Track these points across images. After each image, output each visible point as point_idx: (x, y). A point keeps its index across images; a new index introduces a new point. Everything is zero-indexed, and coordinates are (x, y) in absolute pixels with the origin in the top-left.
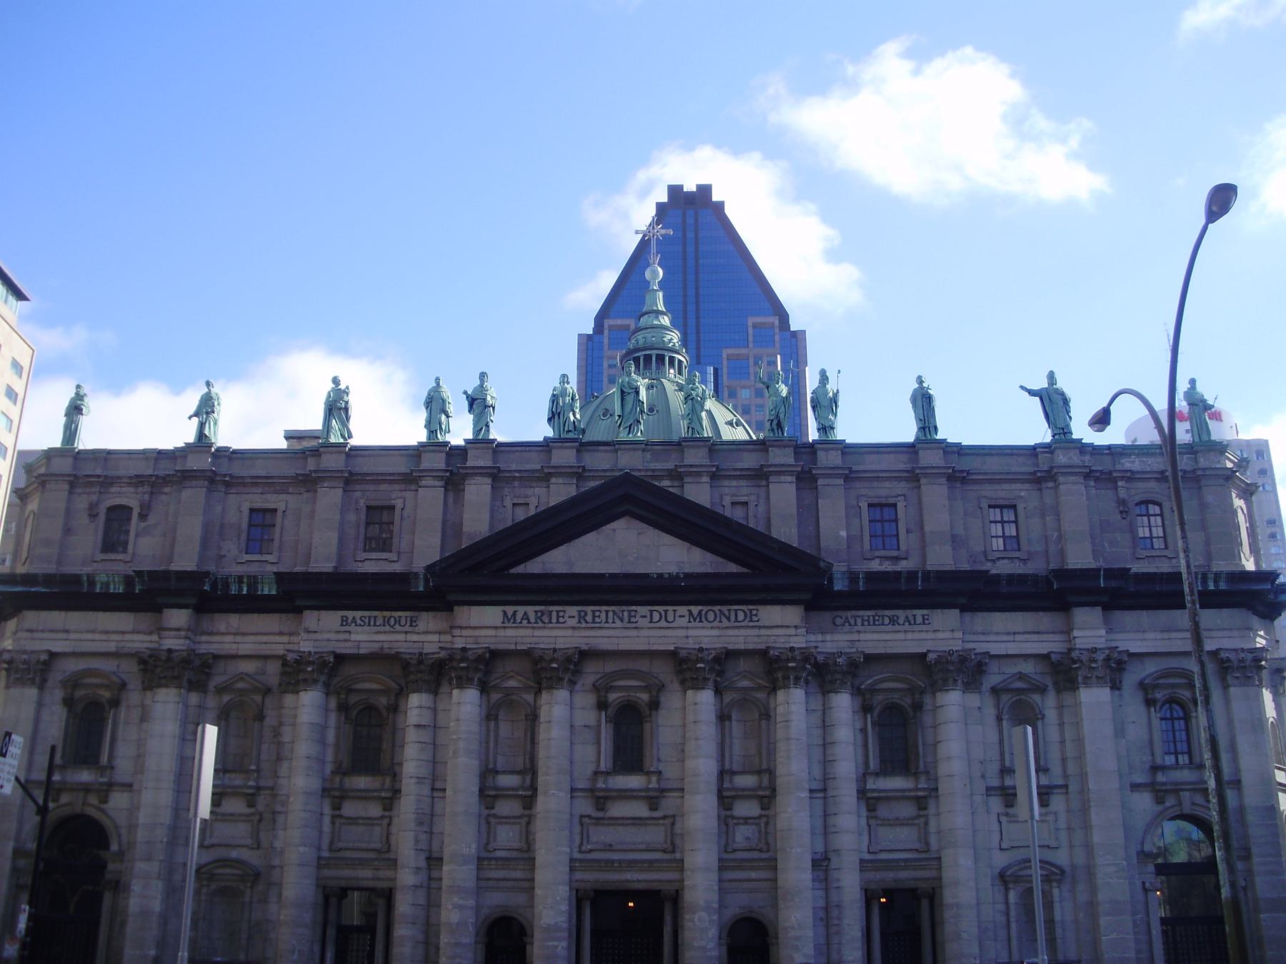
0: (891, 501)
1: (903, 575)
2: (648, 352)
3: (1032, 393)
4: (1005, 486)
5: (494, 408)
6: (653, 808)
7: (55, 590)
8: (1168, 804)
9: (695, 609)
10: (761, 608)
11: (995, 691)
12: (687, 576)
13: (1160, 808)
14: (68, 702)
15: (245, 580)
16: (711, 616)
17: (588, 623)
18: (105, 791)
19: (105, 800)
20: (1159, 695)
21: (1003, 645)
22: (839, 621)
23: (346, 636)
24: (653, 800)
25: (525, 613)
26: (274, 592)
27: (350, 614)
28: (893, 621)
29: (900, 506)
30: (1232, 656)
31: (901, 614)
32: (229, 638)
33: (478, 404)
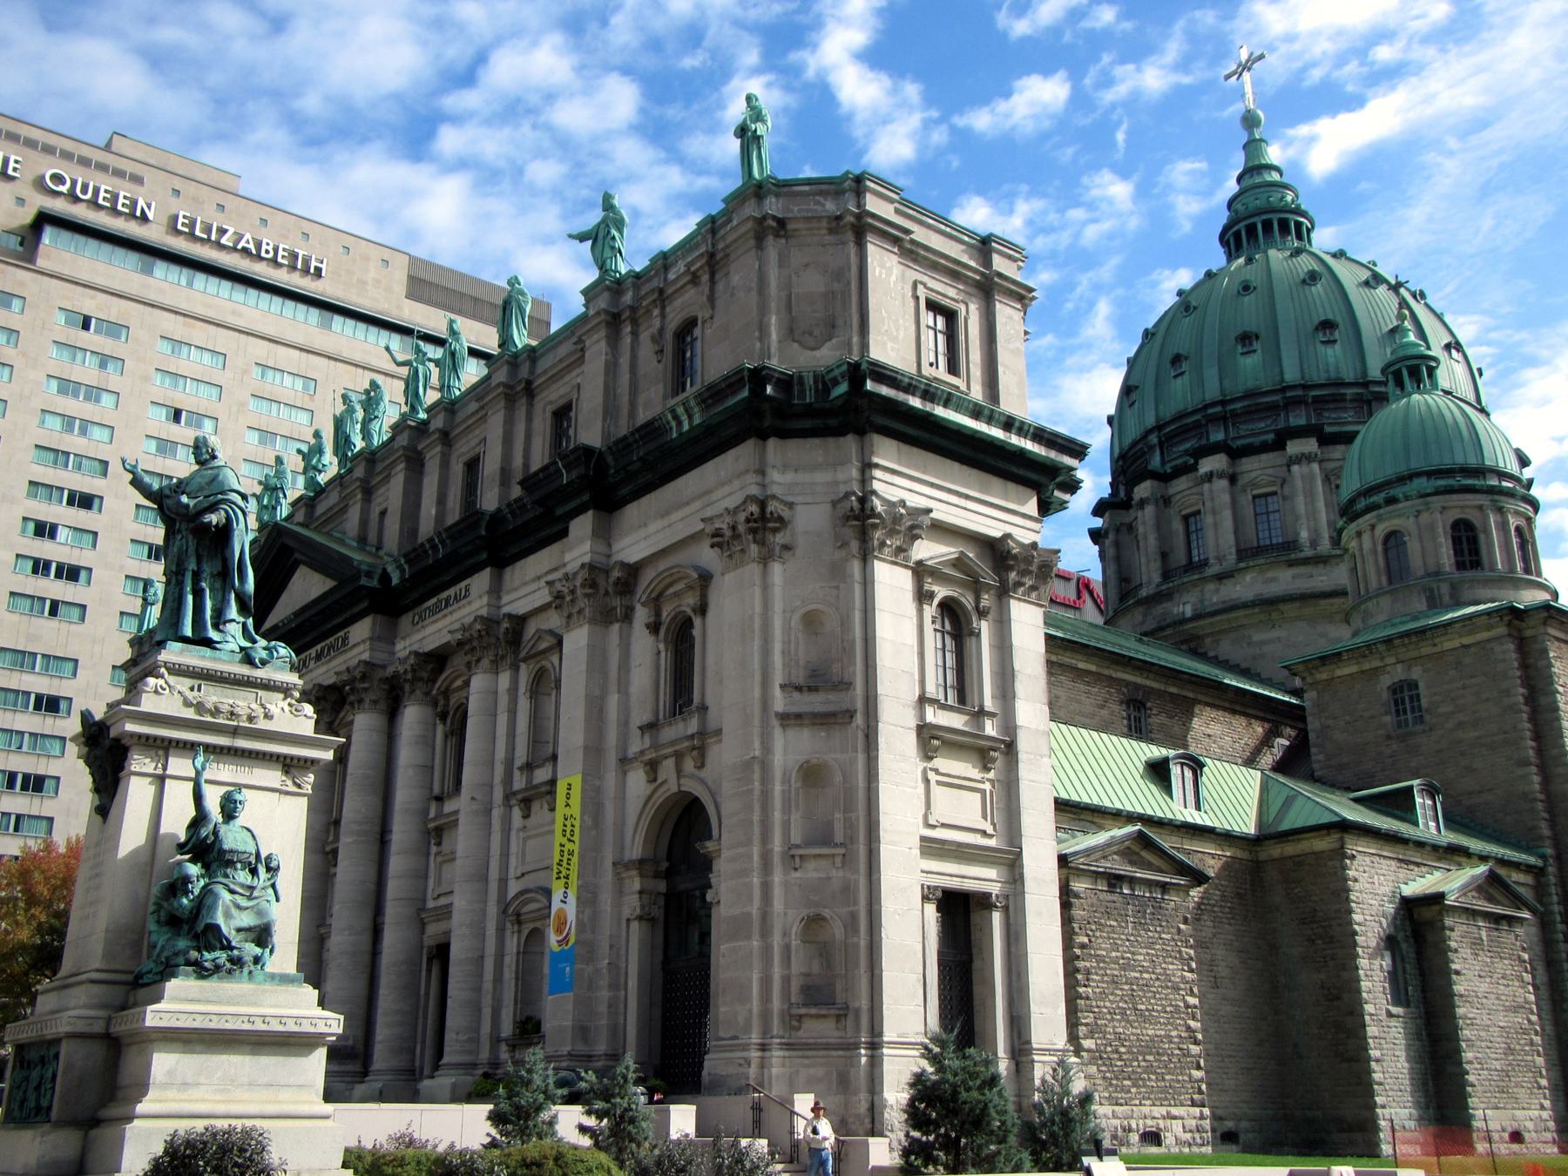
0: (477, 450)
1: (427, 546)
2: (1236, 228)
3: (582, 238)
4: (567, 378)
5: (282, 488)
8: (659, 781)
9: (319, 647)
10: (350, 629)
12: (297, 614)
13: (653, 786)
20: (667, 613)
21: (530, 598)
22: (417, 618)
30: (723, 524)
31: (451, 592)
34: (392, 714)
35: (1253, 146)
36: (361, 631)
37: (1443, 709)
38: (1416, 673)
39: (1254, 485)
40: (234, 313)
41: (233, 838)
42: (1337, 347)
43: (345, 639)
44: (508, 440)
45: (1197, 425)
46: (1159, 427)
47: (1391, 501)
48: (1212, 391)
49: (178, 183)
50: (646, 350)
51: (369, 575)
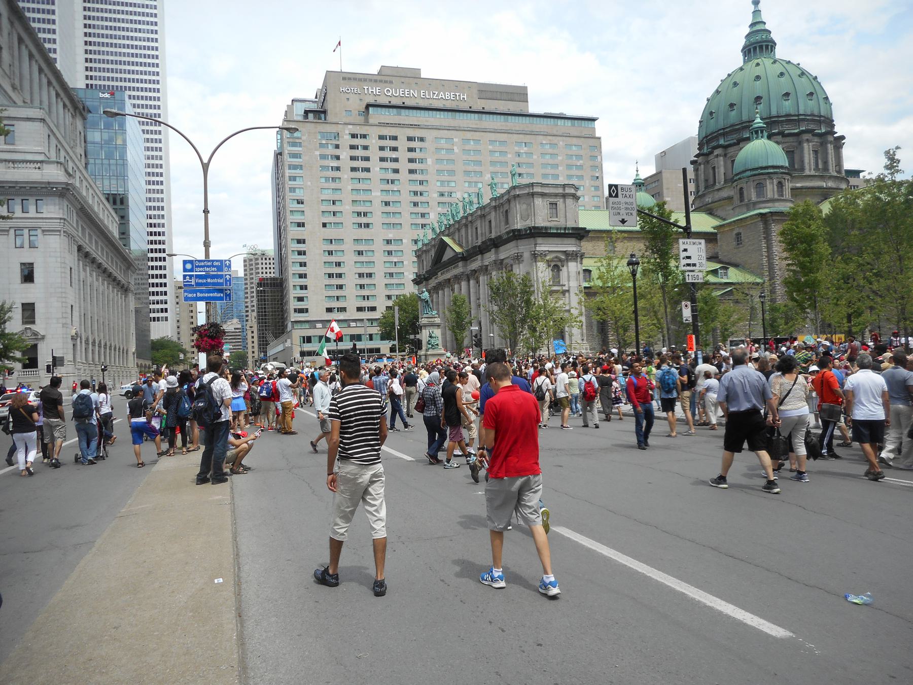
34: (469, 281)
35: (757, 12)
36: (460, 264)
37: (746, 241)
38: (741, 231)
39: (731, 157)
40: (427, 121)
41: (433, 335)
42: (762, 105)
44: (481, 227)
45: (716, 137)
46: (706, 137)
47: (740, 179)
48: (721, 125)
49: (403, 80)
50: (501, 214)
51: (460, 254)
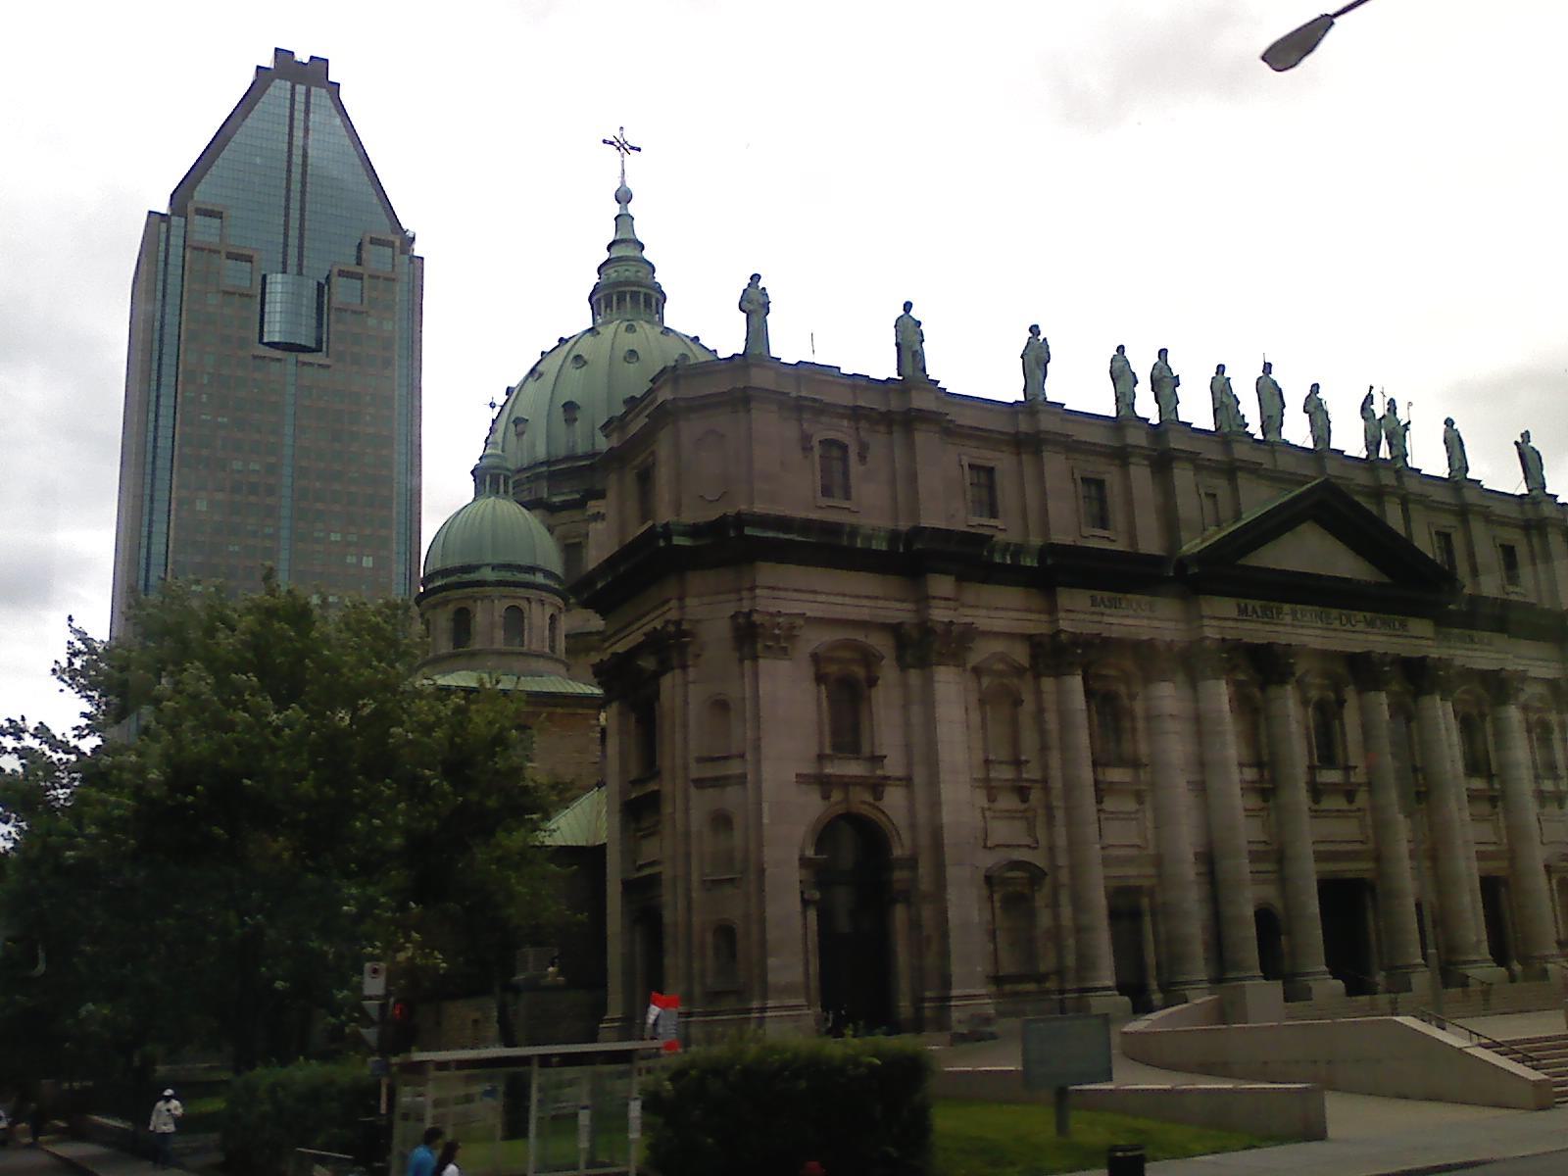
0: (1447, 530)
6: (1351, 801)
7: (811, 540)
9: (1368, 615)
11: (1525, 708)
14: (820, 678)
15: (1012, 548)
16: (1378, 623)
17: (1298, 619)
18: (877, 787)
19: (879, 797)
23: (1096, 618)
24: (1350, 795)
25: (1253, 607)
26: (1036, 565)
27: (1098, 594)
28: (1472, 641)
29: (1454, 537)
32: (983, 612)
33: (1165, 382)
43: (1403, 626)
